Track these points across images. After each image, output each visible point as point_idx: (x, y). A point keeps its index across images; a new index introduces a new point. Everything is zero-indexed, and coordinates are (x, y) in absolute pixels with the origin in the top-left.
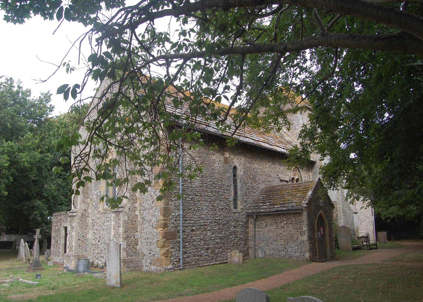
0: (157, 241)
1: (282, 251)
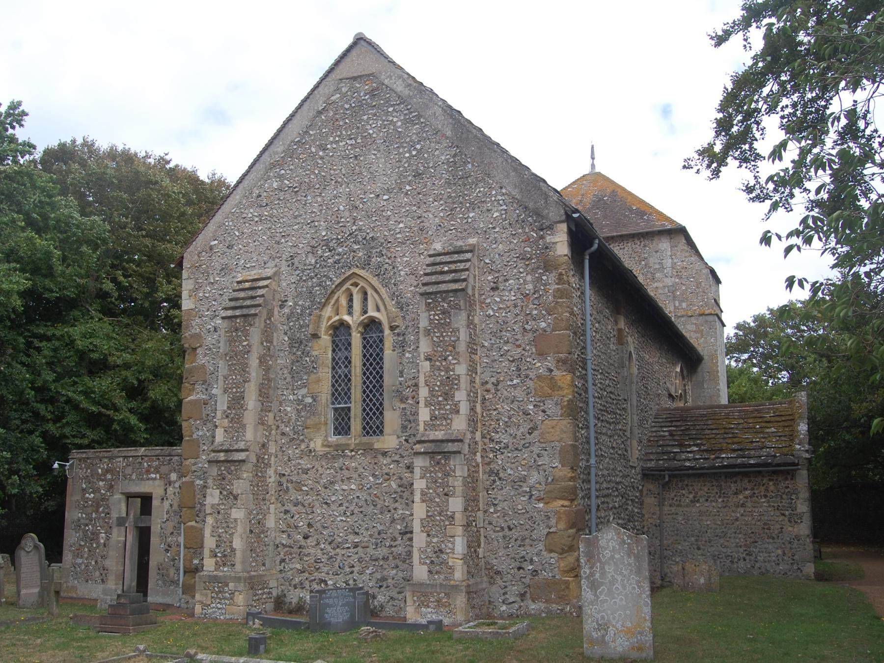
0: (549, 533)
1: (739, 560)
